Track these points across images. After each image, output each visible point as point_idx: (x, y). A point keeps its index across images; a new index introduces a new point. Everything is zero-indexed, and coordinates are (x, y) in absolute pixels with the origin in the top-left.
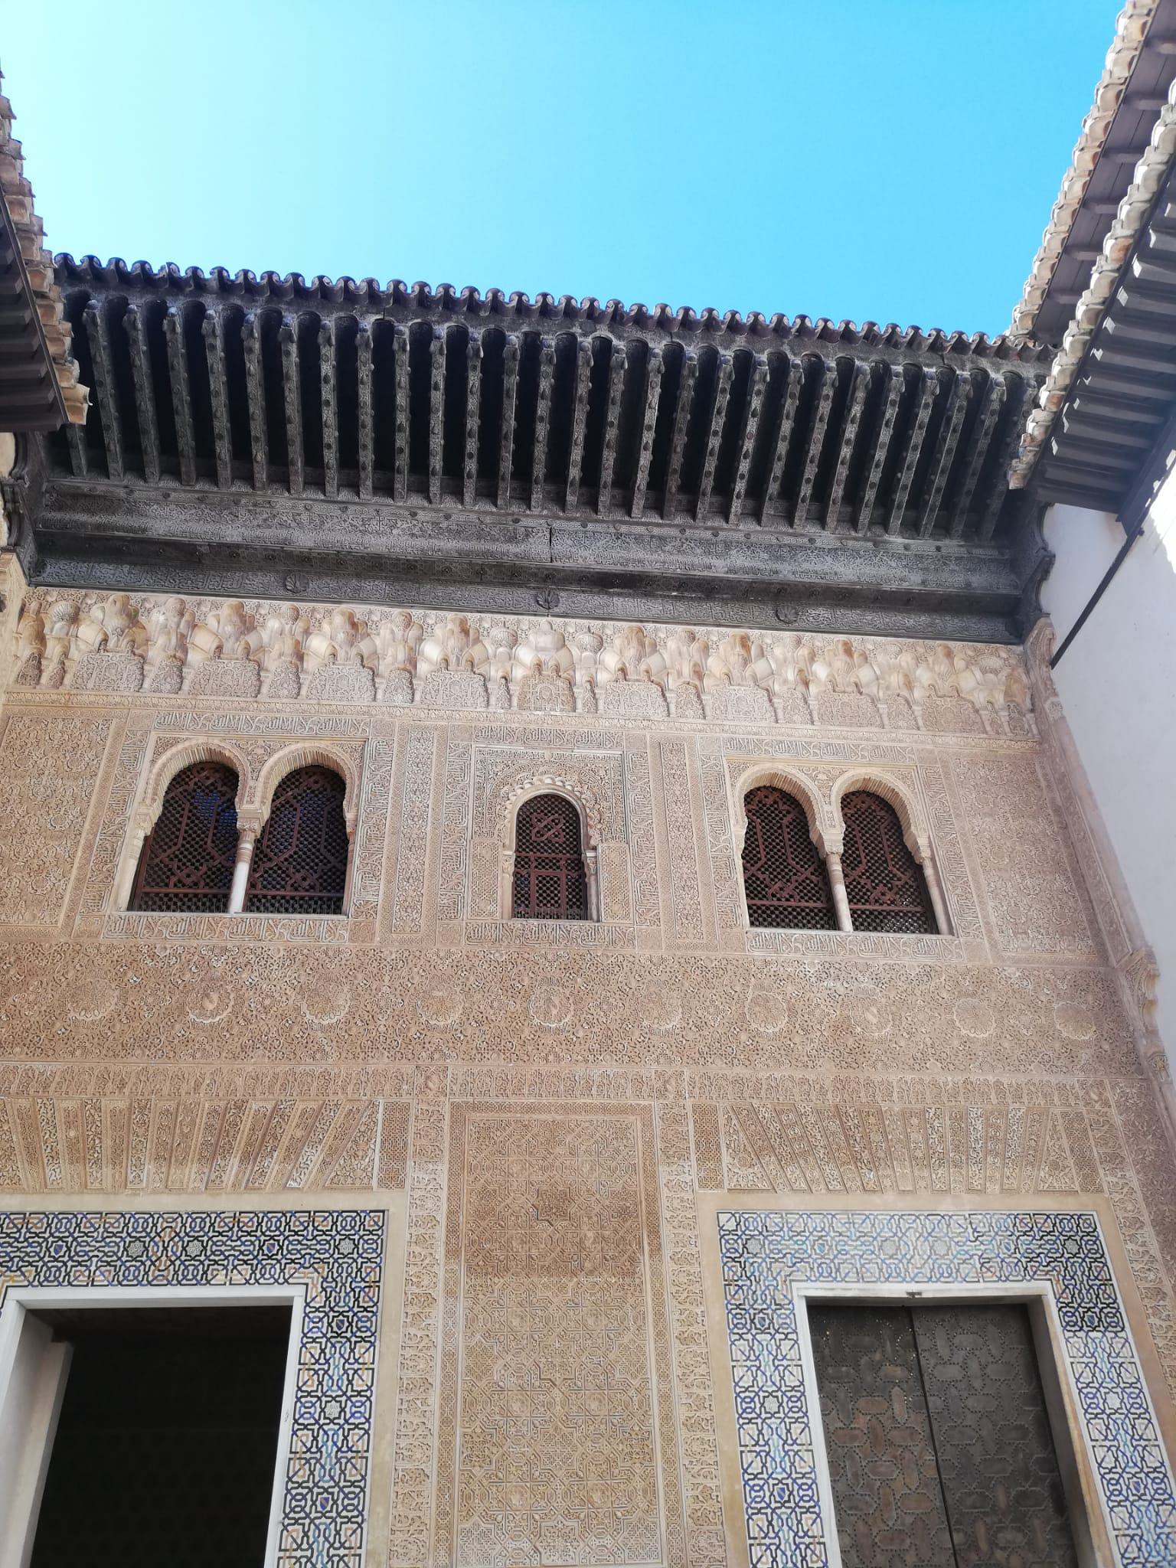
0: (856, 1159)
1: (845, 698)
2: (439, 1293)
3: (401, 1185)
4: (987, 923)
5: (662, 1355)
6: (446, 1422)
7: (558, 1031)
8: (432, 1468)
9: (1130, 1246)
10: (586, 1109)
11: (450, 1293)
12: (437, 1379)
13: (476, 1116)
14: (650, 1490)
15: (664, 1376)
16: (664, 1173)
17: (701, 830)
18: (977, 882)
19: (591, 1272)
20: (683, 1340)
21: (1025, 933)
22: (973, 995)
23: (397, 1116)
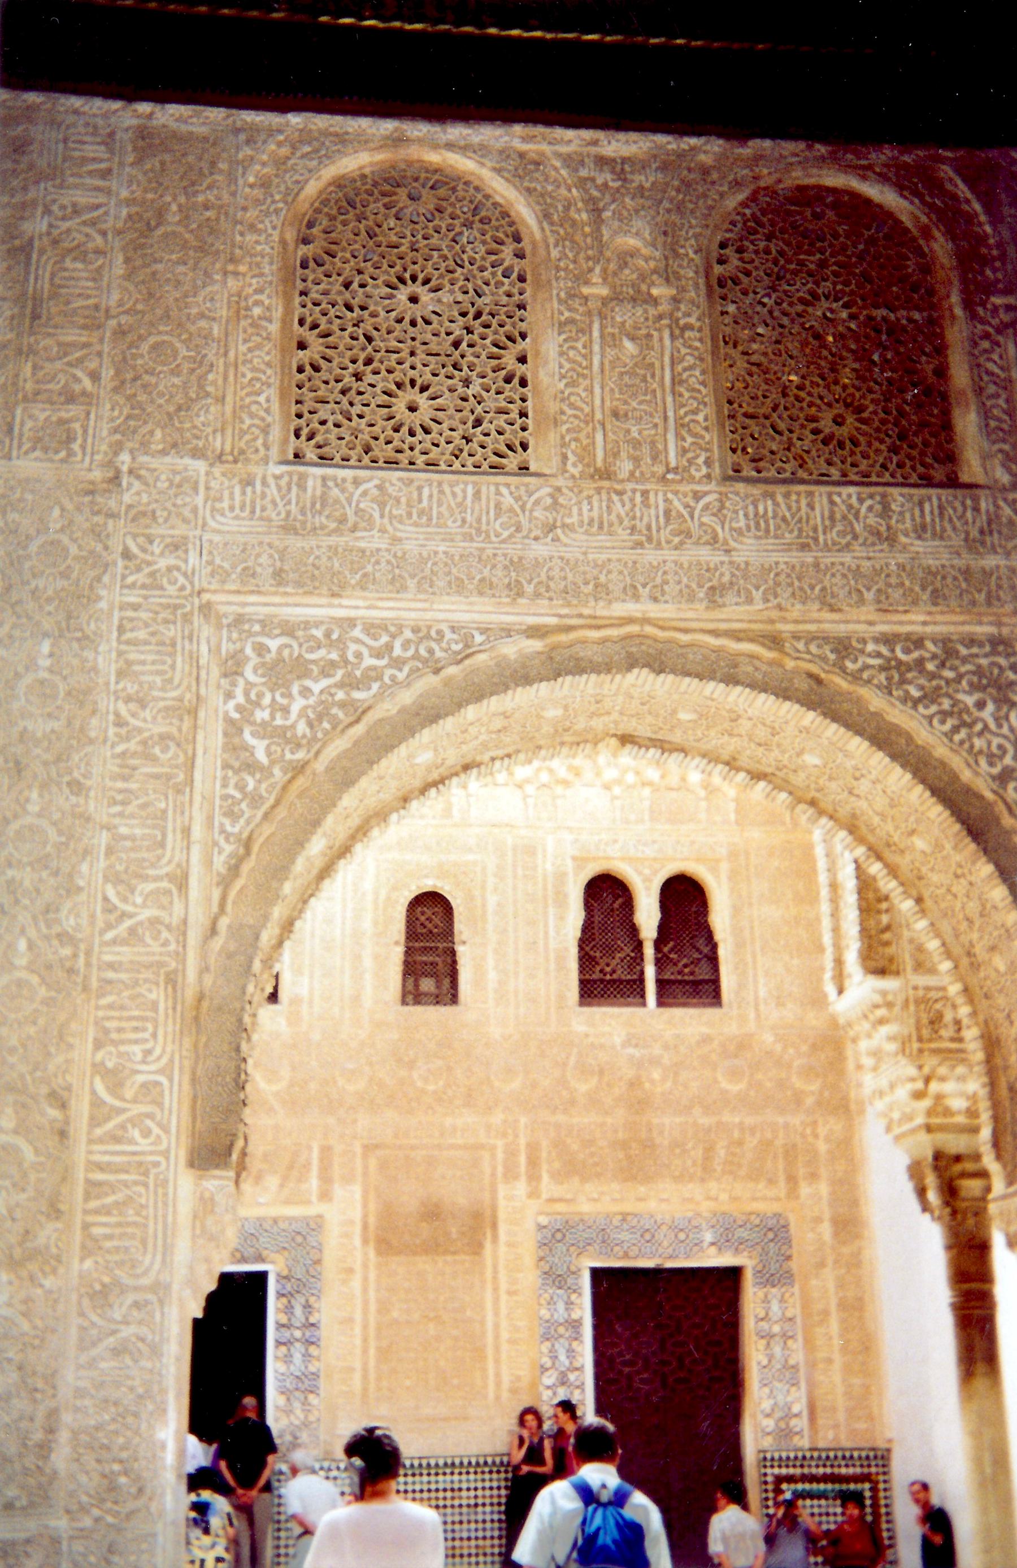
0: (634, 1178)
1: (674, 795)
2: (358, 1267)
3: (331, 1200)
4: (756, 998)
5: (496, 1300)
6: (365, 1340)
7: (435, 1092)
8: (358, 1365)
9: (810, 1235)
10: (452, 1147)
11: (365, 1266)
12: (358, 1316)
13: (379, 1152)
14: (485, 1378)
15: (496, 1314)
16: (502, 1190)
17: (546, 925)
18: (755, 962)
19: (454, 1253)
20: (510, 1293)
21: (783, 1005)
22: (736, 1056)
23: (326, 1151)
